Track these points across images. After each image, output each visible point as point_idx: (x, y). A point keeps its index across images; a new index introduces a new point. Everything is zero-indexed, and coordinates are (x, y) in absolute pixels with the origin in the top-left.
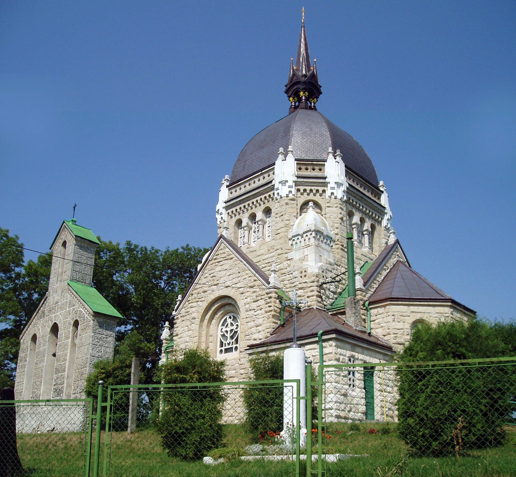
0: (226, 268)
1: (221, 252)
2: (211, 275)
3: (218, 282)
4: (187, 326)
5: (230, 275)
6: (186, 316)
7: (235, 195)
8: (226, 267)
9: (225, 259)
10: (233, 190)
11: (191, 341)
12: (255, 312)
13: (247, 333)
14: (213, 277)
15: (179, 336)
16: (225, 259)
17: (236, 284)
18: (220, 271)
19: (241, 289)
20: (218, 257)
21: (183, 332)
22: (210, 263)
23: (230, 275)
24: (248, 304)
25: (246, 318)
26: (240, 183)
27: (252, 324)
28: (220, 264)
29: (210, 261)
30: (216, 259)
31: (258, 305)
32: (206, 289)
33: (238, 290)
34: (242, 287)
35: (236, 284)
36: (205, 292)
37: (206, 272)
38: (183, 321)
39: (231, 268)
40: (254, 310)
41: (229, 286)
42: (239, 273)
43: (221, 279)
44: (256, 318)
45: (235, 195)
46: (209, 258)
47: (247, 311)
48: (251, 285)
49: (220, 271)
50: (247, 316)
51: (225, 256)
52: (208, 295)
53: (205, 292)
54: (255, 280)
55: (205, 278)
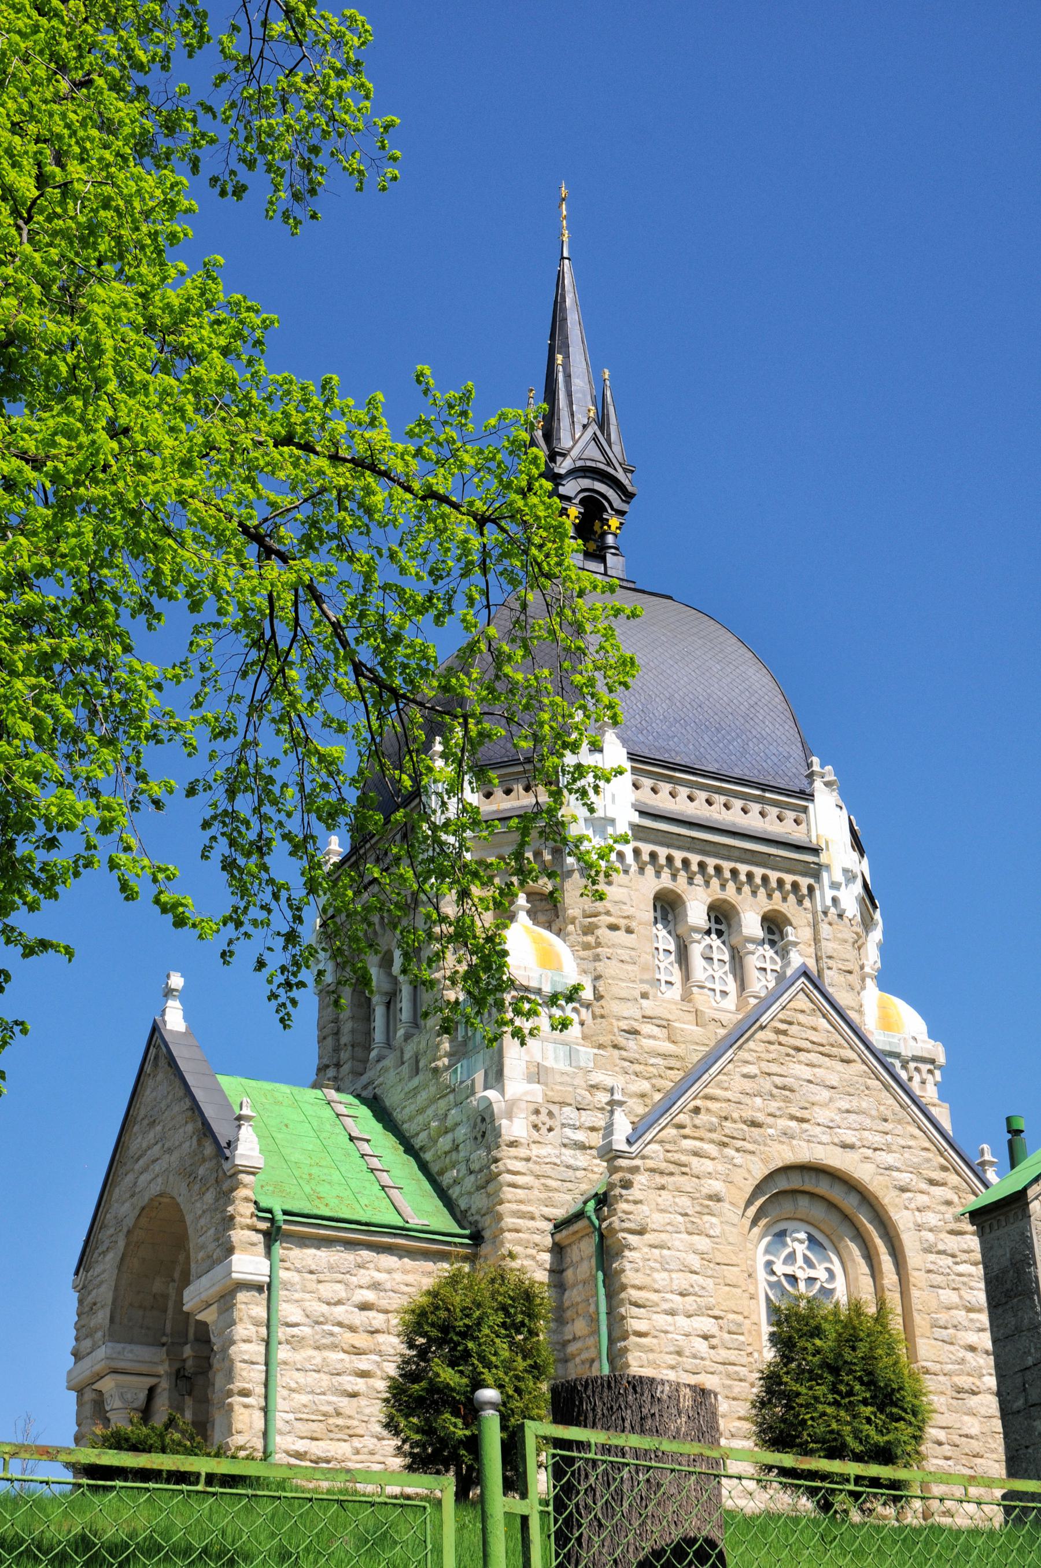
0: (835, 1084)
1: (802, 1018)
2: (778, 1080)
3: (805, 1114)
4: (686, 1215)
5: (848, 1111)
6: (672, 1174)
7: (645, 796)
8: (833, 1079)
9: (821, 1049)
10: (647, 783)
11: (710, 1273)
12: (956, 1263)
13: (943, 1317)
14: (784, 1088)
15: (648, 1237)
16: (821, 1049)
17: (875, 1150)
18: (810, 1081)
19: (895, 1174)
20: (793, 1029)
21: (669, 1228)
22: (760, 1035)
23: (848, 1111)
24: (931, 1230)
25: (929, 1271)
26: (678, 775)
27: (953, 1297)
28: (803, 1056)
29: (762, 1028)
30: (784, 1033)
31: (965, 1247)
32: (760, 1117)
33: (887, 1172)
34: (903, 1168)
35: (875, 1150)
36: (754, 1124)
37: (743, 1055)
38: (663, 1188)
39: (852, 1090)
40: (953, 1256)
41: (851, 1147)
42: (886, 1120)
43: (816, 1109)
44: (964, 1284)
45: (661, 805)
46: (762, 1020)
47: (928, 1250)
48: (937, 1175)
49: (810, 1081)
50: (932, 1267)
51: (824, 1042)
52: (769, 1142)
53: (754, 1124)
54: (944, 1169)
55: (745, 1076)
